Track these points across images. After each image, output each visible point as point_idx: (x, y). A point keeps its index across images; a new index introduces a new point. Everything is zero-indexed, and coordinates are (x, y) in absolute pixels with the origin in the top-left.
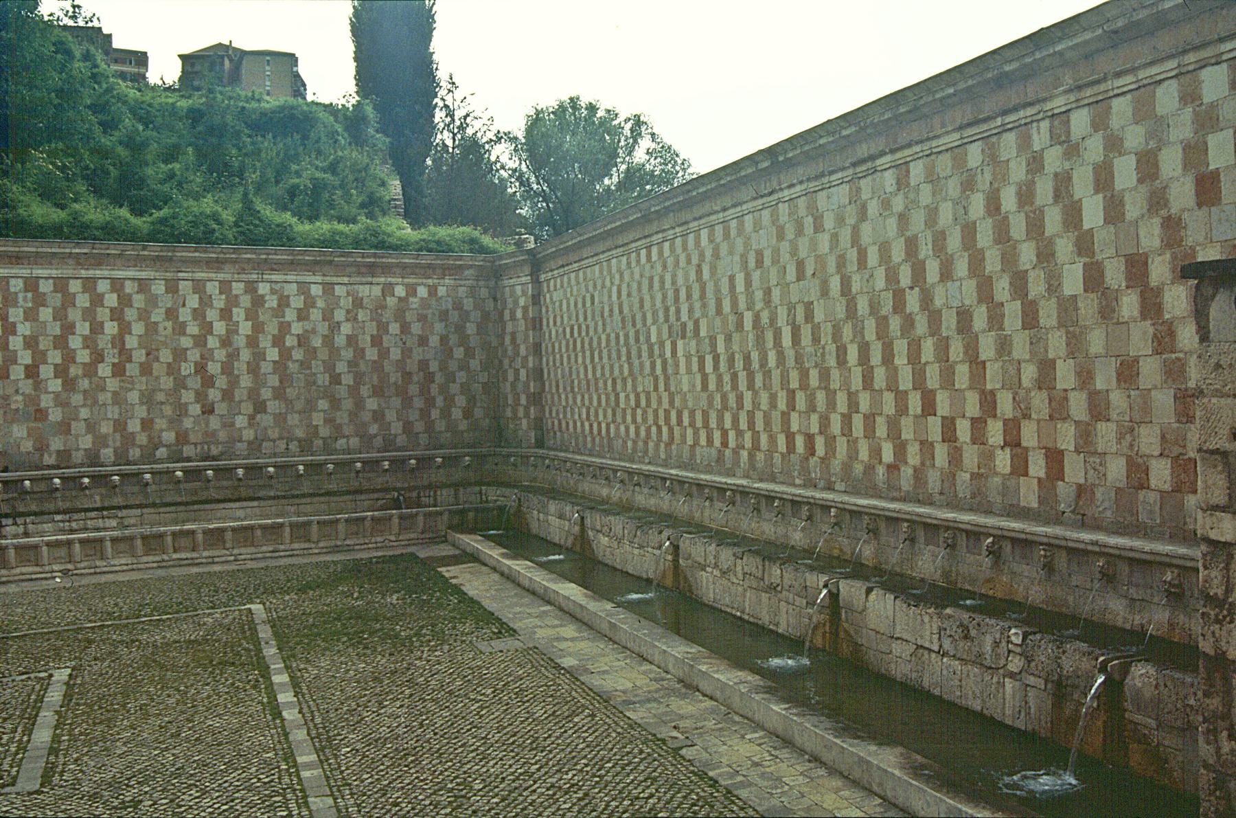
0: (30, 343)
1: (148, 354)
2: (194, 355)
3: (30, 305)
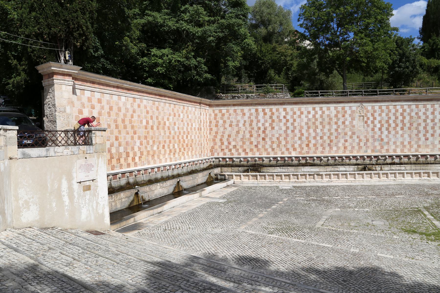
0: (380, 122)
1: (410, 124)
2: (423, 124)
3: (380, 112)
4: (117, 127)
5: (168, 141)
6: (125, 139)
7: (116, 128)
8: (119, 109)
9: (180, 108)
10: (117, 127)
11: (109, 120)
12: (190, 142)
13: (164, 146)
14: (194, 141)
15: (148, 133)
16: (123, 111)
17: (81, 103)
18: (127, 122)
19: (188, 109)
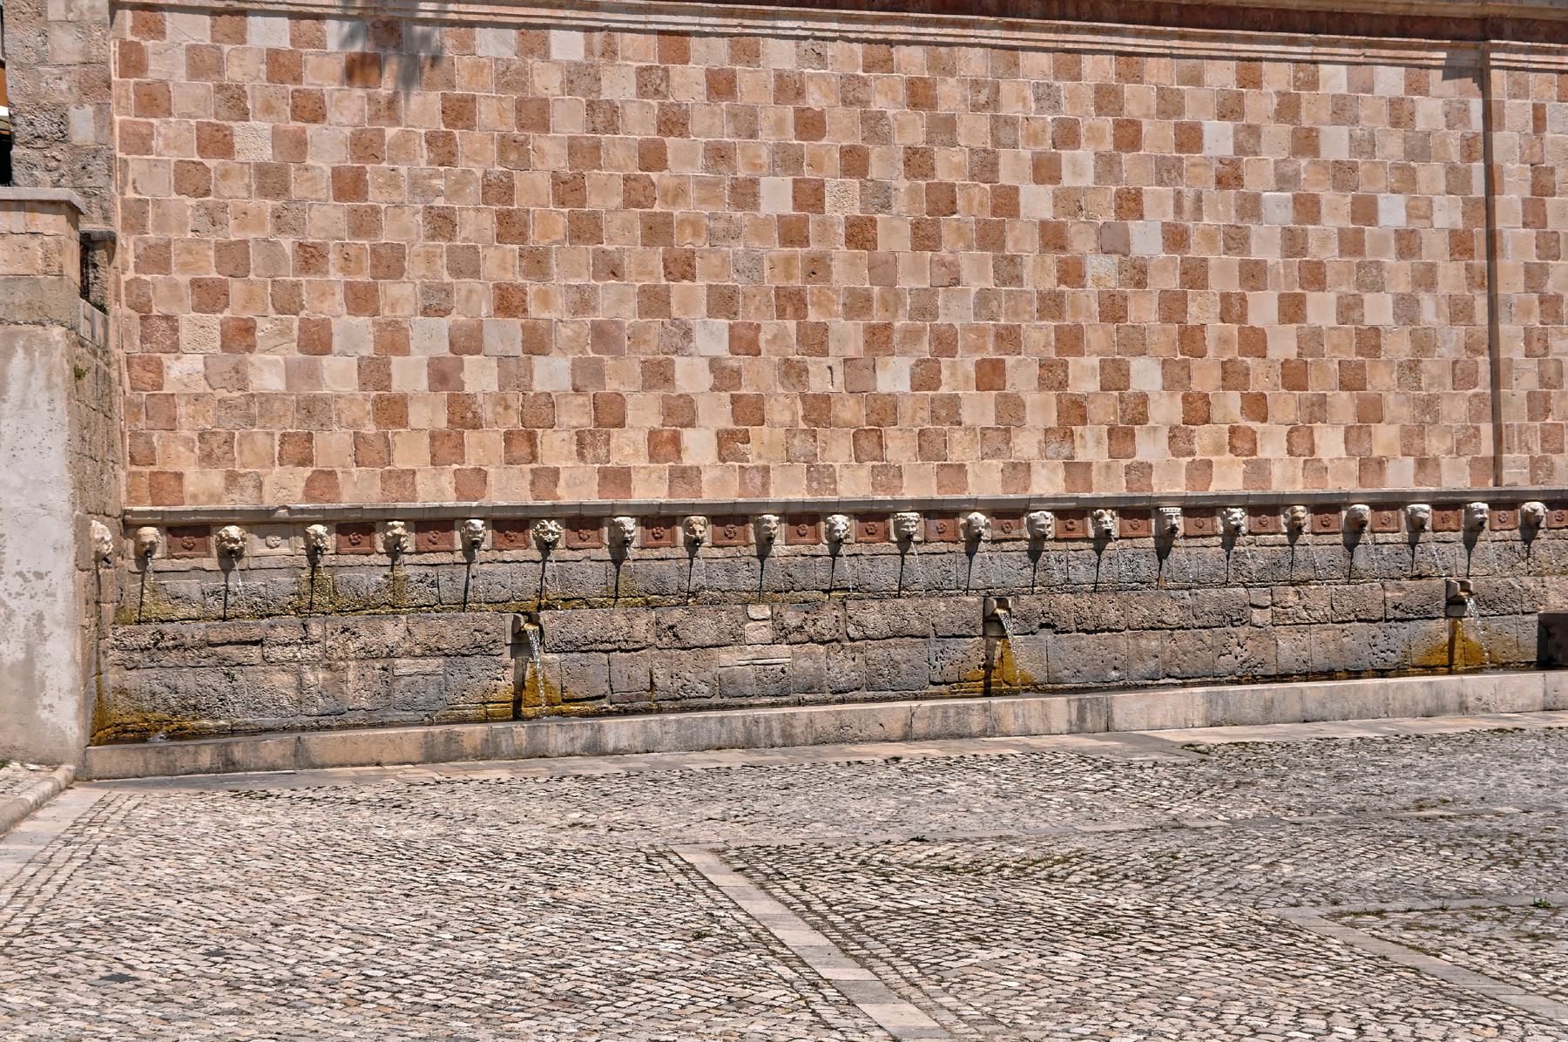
4: (510, 227)
5: (1039, 334)
6: (583, 302)
7: (500, 238)
8: (535, 115)
9: (1196, 80)
10: (510, 227)
11: (439, 183)
12: (1340, 351)
13: (990, 375)
14: (1398, 346)
15: (817, 268)
16: (569, 121)
17: (220, 88)
18: (604, 197)
19: (1313, 84)
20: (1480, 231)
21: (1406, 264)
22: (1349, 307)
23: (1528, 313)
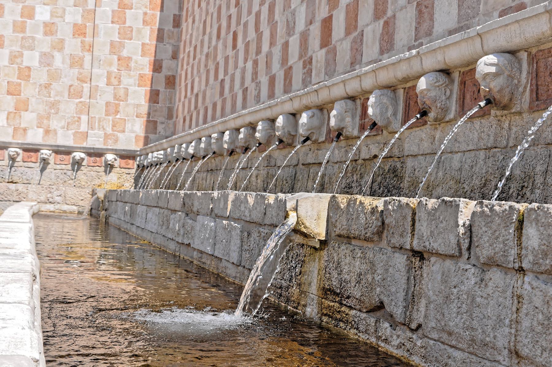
20: (89, 25)
21: (49, 38)
22: (15, 57)
23: (111, 64)
